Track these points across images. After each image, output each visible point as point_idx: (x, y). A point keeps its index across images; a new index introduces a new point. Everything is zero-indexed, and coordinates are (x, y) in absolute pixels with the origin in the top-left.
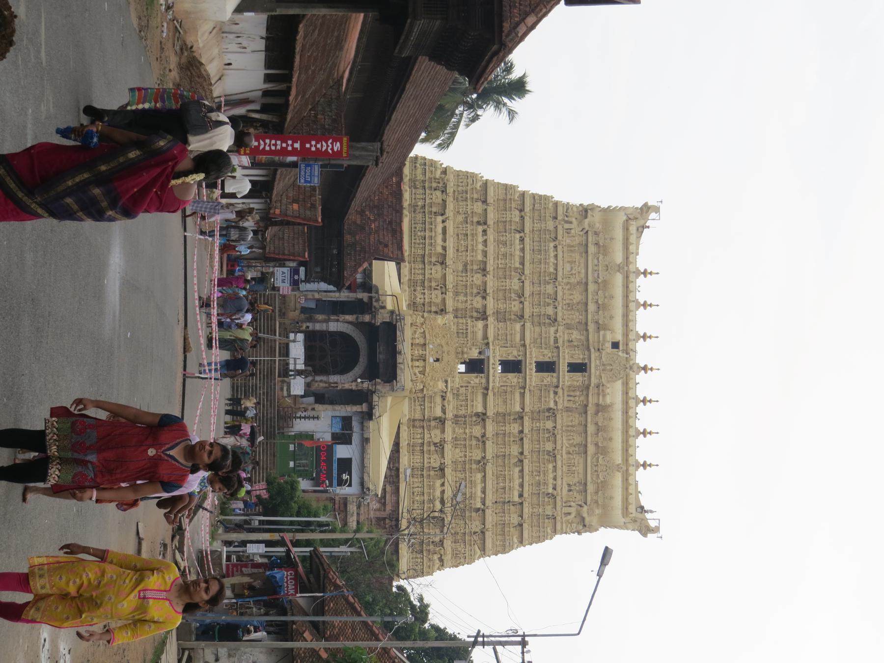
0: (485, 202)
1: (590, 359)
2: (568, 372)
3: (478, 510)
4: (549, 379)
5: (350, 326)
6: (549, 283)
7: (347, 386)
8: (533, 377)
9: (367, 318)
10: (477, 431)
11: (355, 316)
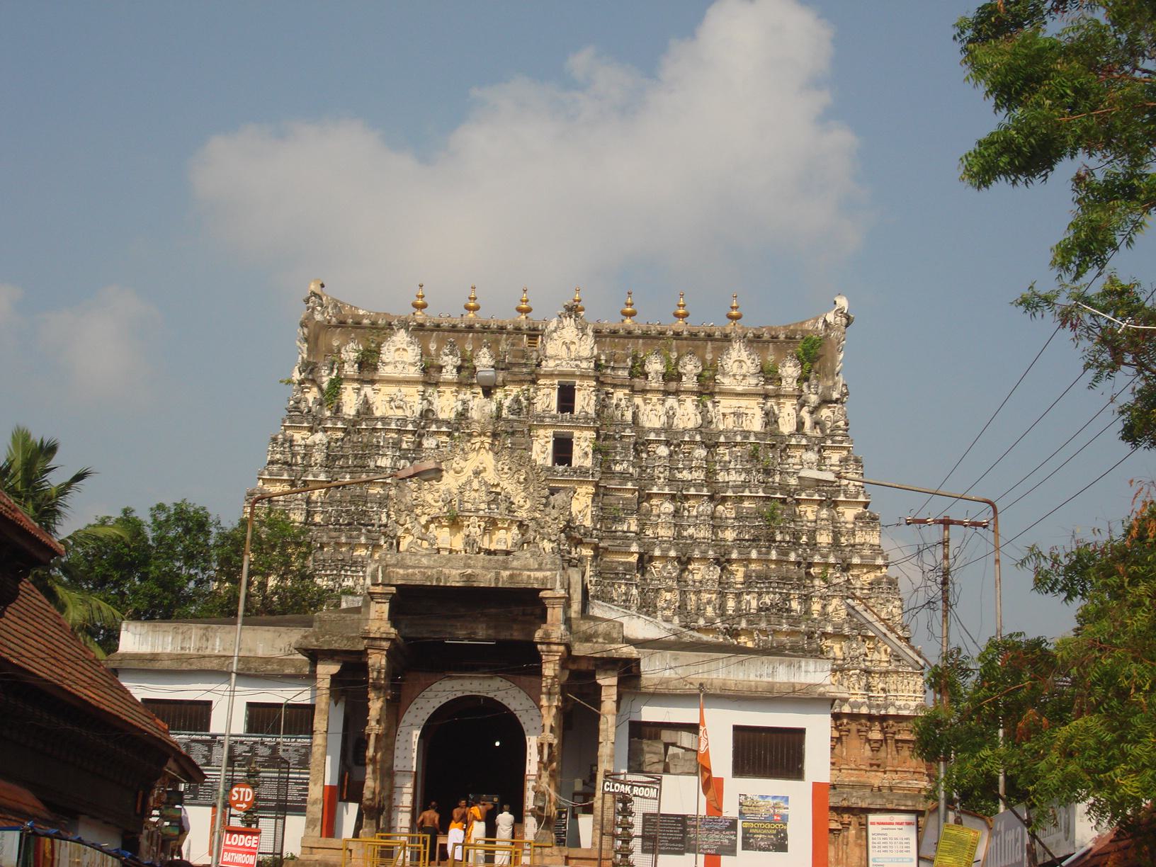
1: (550, 375)
2: (572, 411)
4: (584, 445)
5: (407, 718)
6: (420, 444)
7: (549, 719)
9: (377, 660)
11: (372, 695)
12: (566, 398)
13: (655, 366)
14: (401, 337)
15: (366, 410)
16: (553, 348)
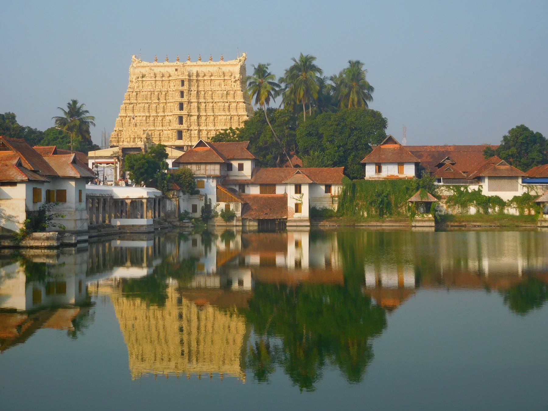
0: (126, 117)
3: (231, 118)
8: (185, 99)
10: (203, 118)
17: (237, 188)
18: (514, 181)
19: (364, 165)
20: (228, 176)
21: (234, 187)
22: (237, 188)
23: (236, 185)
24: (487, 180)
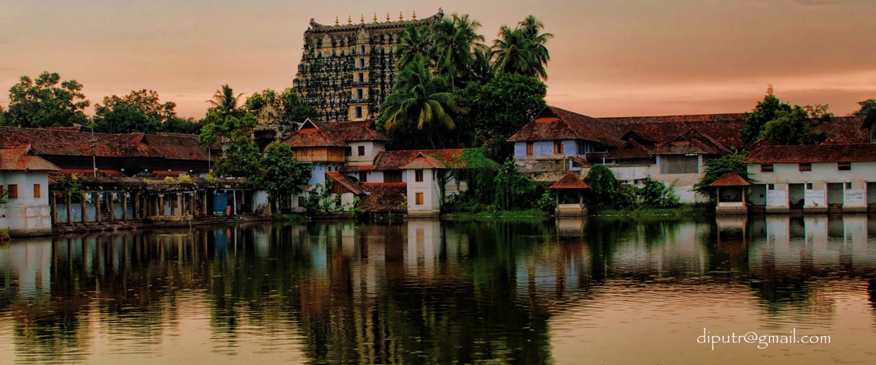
12: (363, 47)
13: (387, 37)
14: (326, 36)
15: (320, 55)
16: (359, 37)
17: (357, 177)
18: (692, 162)
19: (514, 143)
20: (347, 161)
21: (354, 176)
22: (357, 177)
23: (356, 173)
24: (658, 159)
